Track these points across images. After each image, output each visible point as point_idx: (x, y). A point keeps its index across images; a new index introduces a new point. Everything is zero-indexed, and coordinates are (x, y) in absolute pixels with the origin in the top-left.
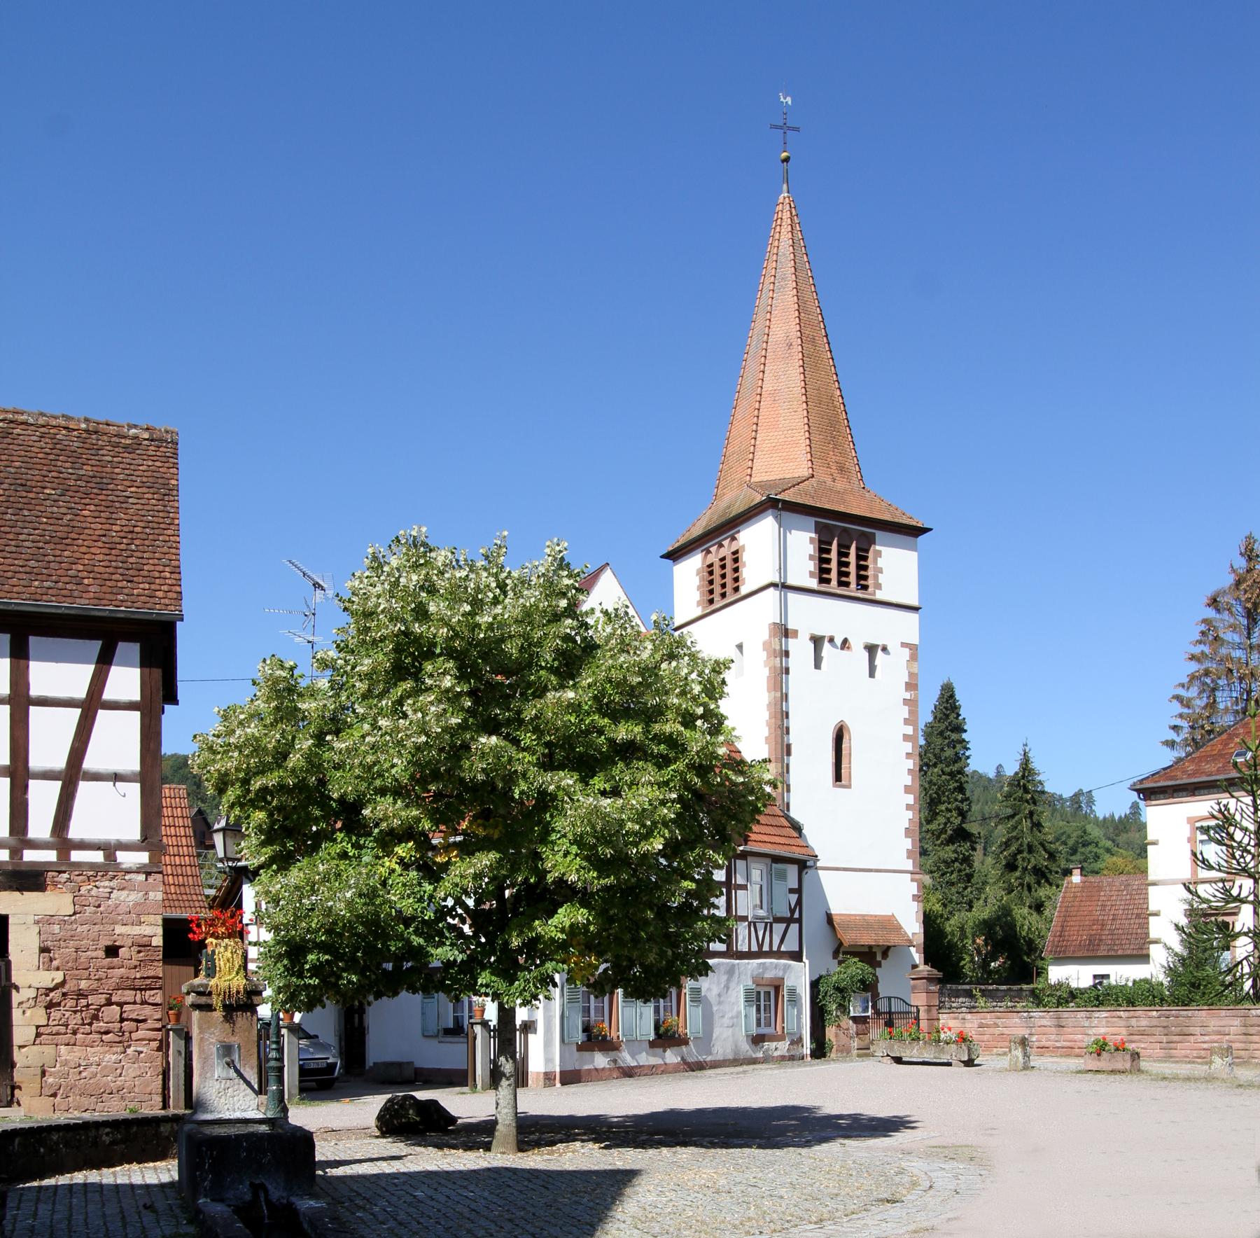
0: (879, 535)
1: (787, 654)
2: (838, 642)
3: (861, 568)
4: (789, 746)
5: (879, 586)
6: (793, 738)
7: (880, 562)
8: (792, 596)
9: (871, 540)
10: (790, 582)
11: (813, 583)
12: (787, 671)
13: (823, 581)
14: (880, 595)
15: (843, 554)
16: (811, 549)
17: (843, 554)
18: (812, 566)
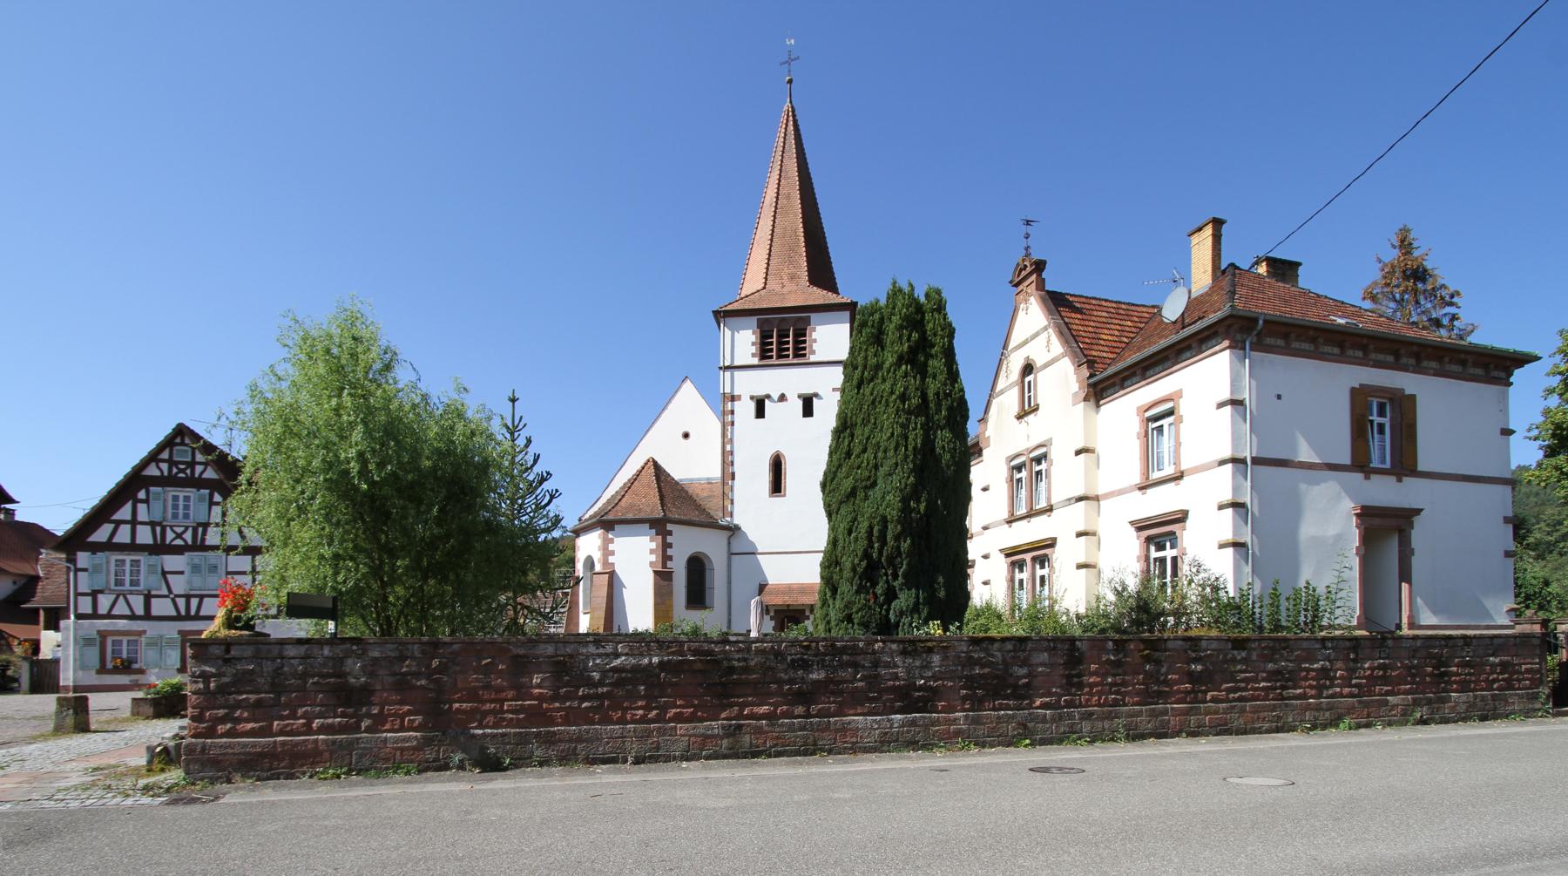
0: (814, 316)
1: (732, 412)
2: (775, 396)
3: (796, 342)
4: (733, 475)
5: (813, 352)
6: (737, 468)
7: (814, 335)
8: (737, 374)
9: (807, 321)
10: (737, 363)
11: (755, 361)
12: (733, 424)
13: (763, 357)
14: (813, 358)
15: (783, 335)
16: (753, 338)
17: (783, 335)
18: (753, 349)
